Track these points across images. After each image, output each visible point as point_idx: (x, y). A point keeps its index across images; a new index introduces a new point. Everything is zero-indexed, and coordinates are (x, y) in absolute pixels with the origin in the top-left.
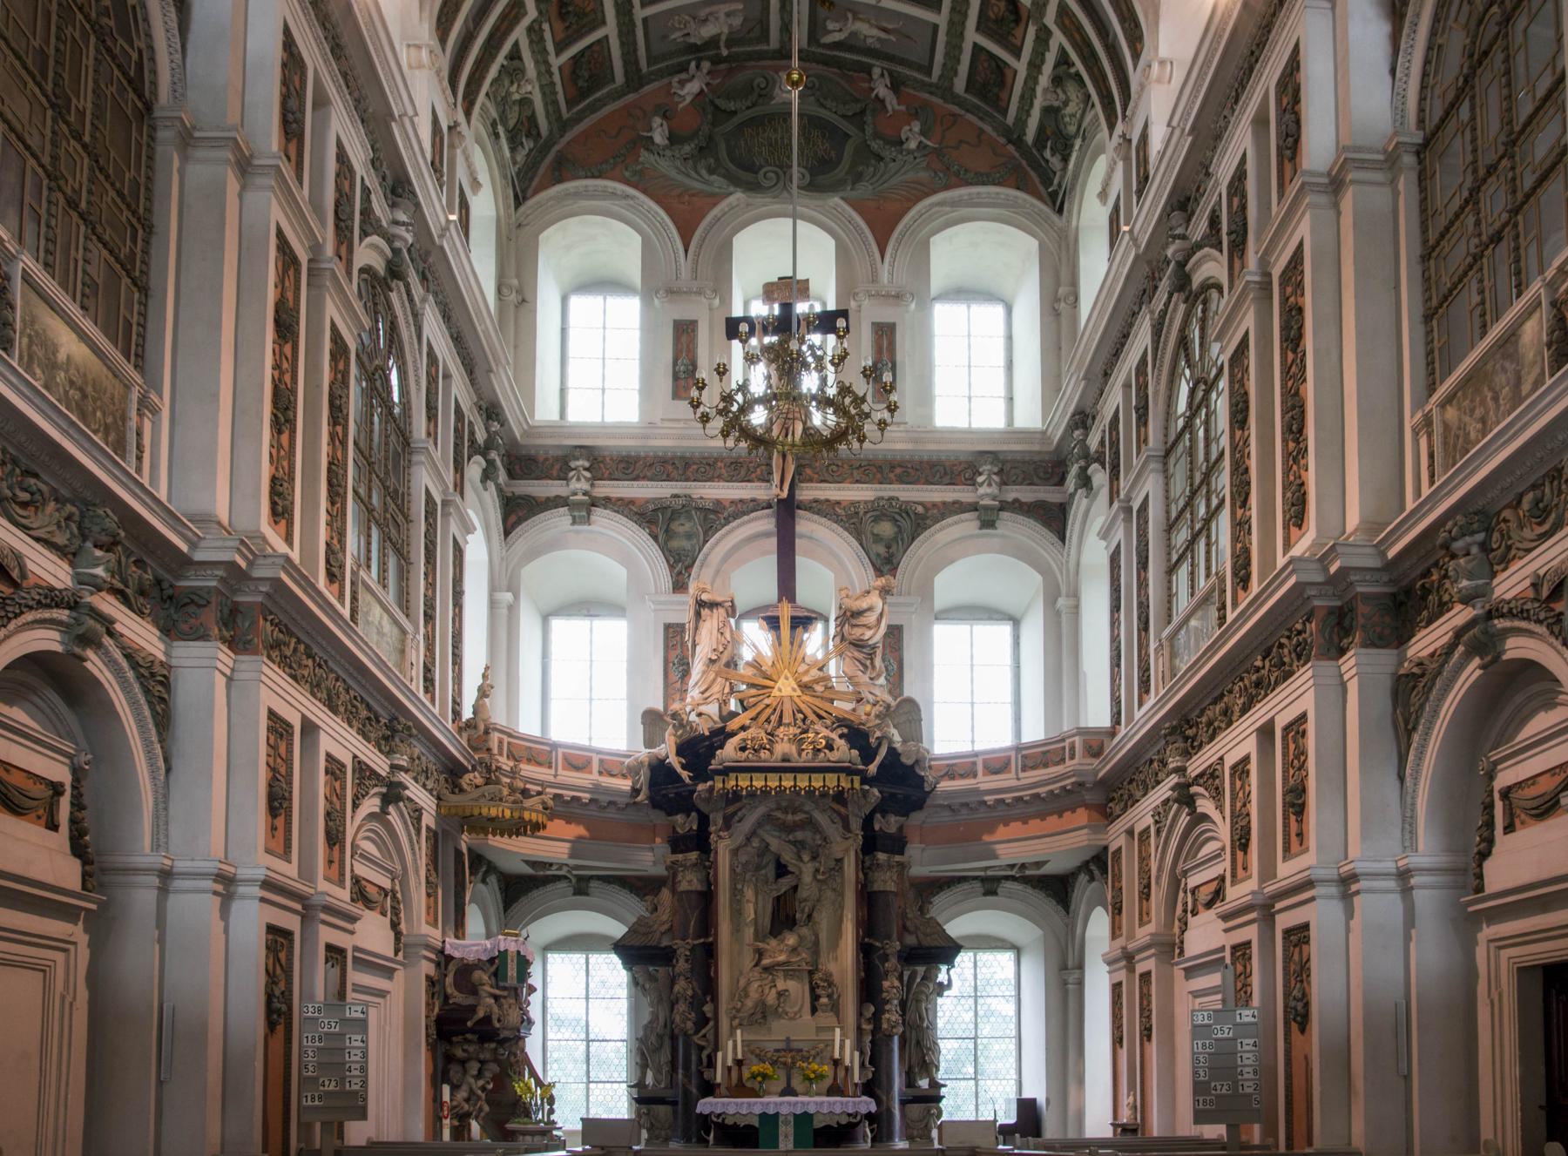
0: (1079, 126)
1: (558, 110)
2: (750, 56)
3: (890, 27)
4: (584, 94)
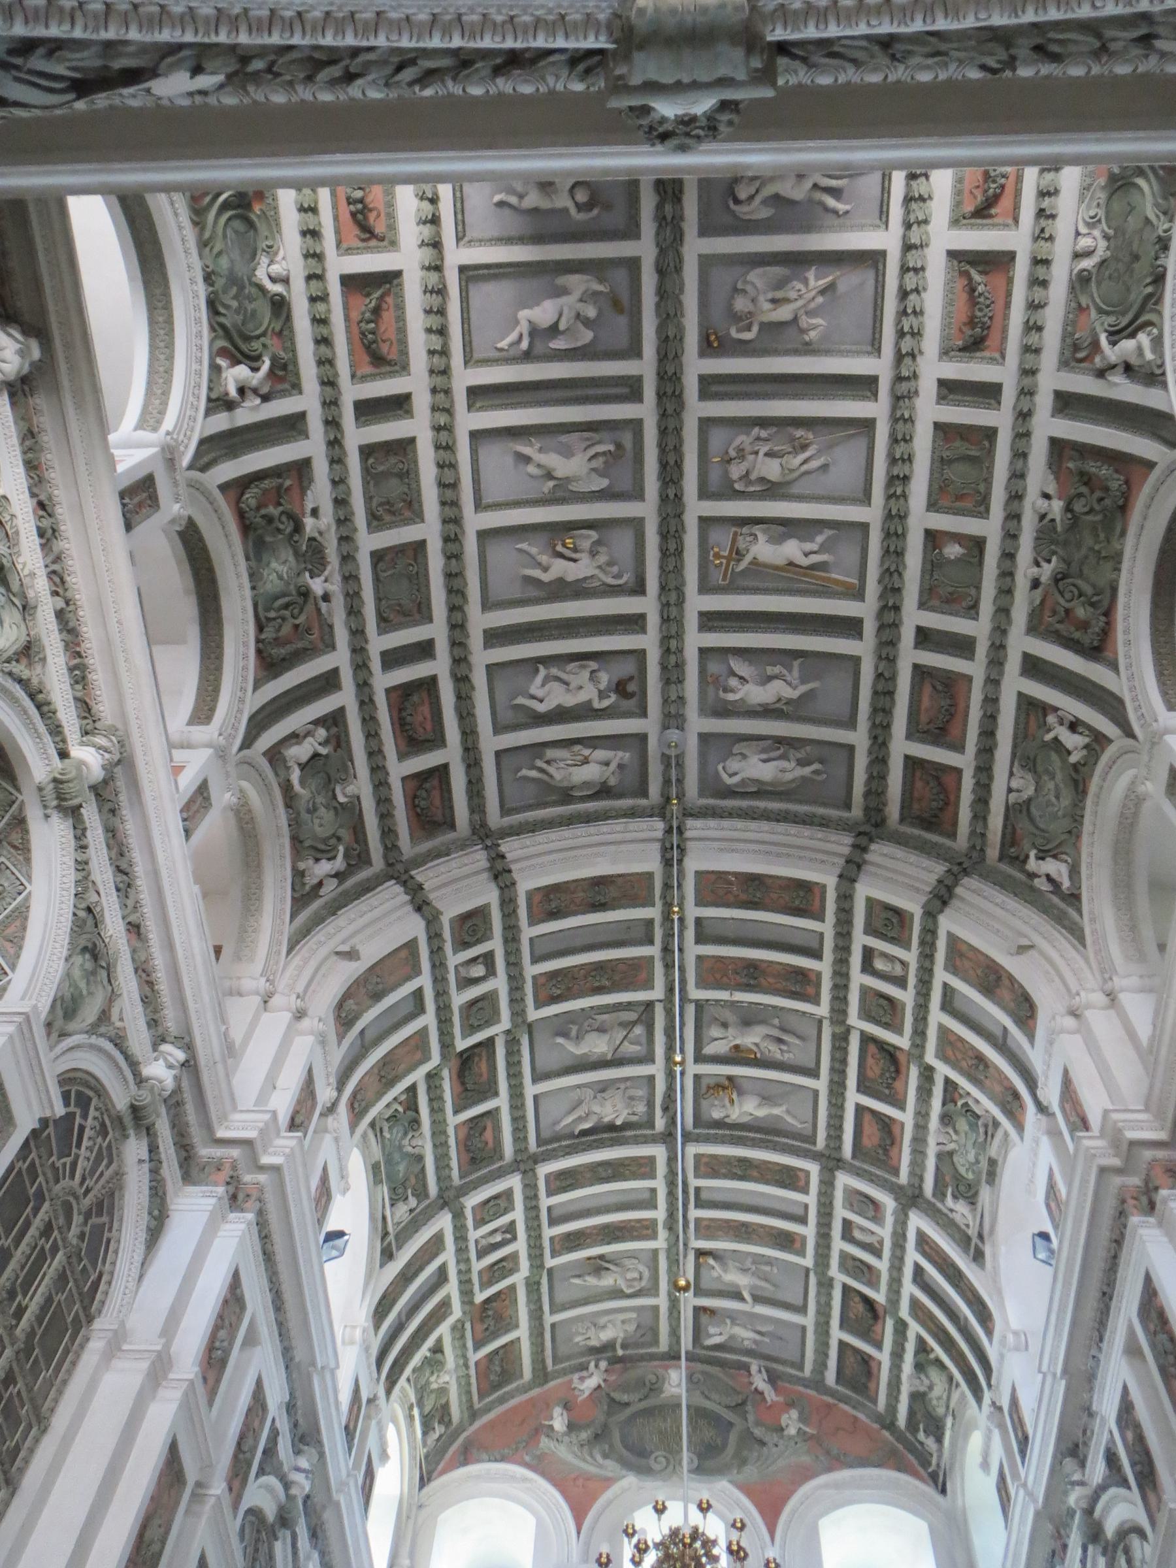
0: (948, 1407)
1: (470, 1400)
2: (642, 1358)
3: (764, 1329)
4: (496, 1387)
